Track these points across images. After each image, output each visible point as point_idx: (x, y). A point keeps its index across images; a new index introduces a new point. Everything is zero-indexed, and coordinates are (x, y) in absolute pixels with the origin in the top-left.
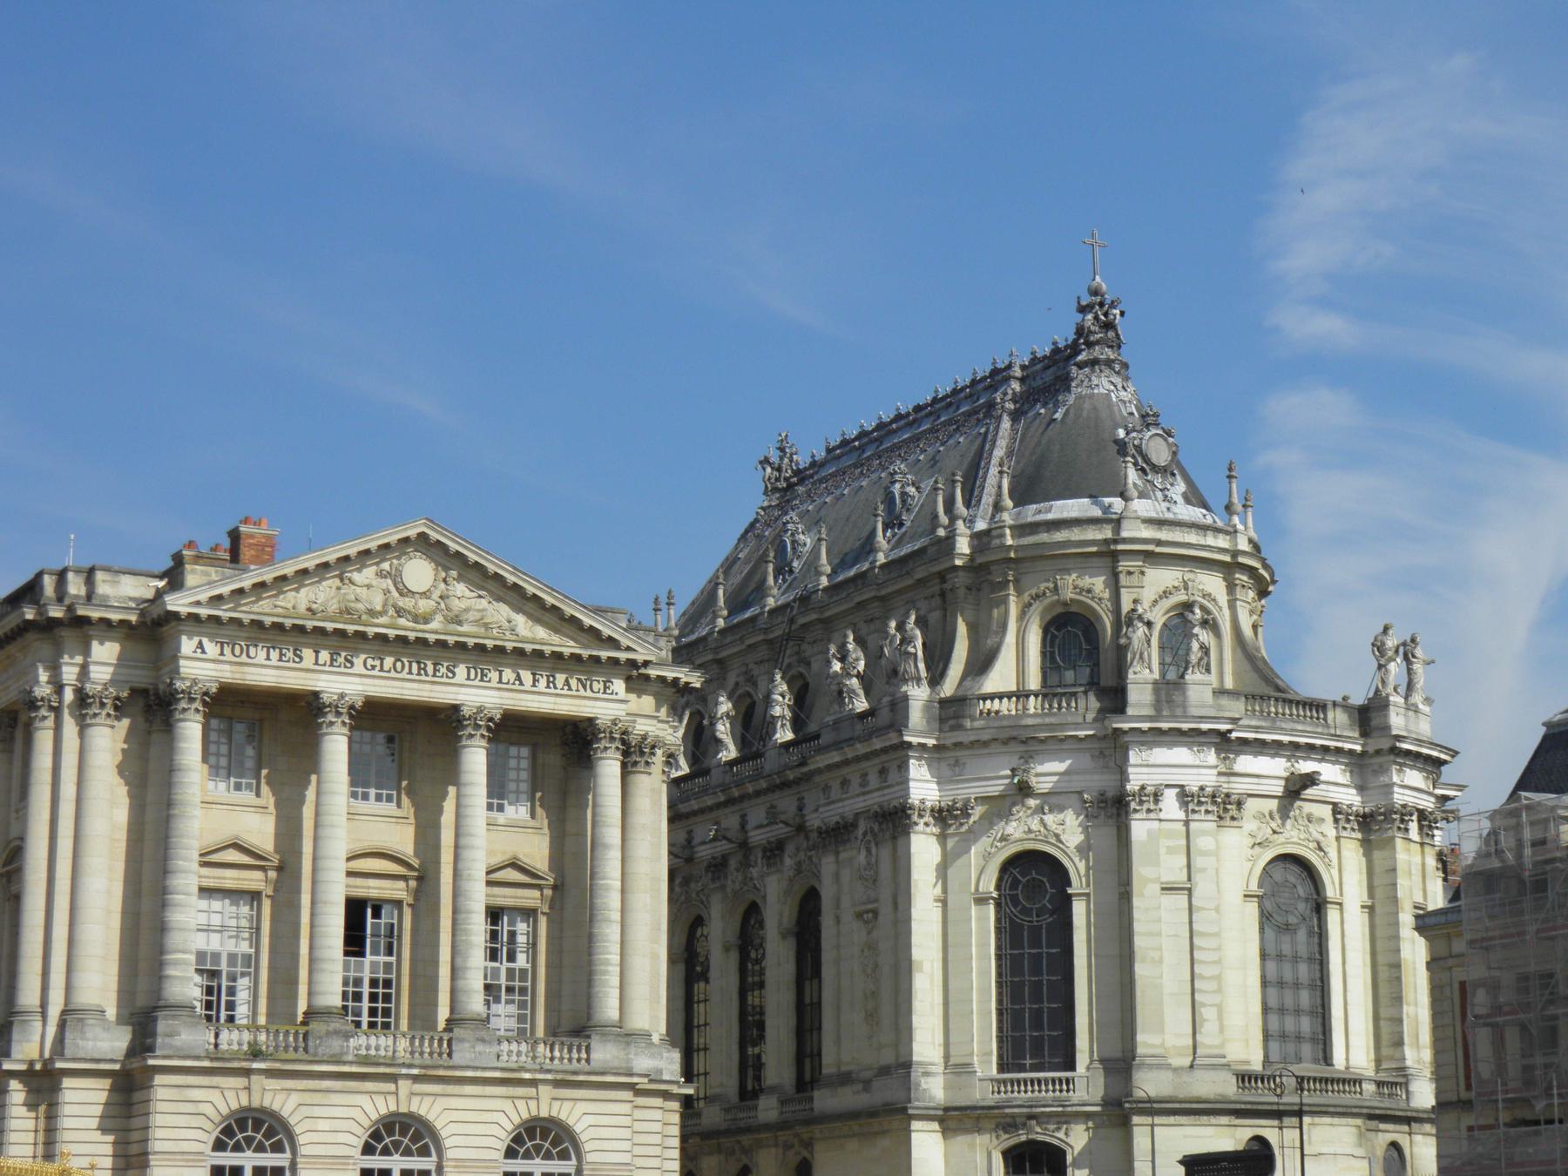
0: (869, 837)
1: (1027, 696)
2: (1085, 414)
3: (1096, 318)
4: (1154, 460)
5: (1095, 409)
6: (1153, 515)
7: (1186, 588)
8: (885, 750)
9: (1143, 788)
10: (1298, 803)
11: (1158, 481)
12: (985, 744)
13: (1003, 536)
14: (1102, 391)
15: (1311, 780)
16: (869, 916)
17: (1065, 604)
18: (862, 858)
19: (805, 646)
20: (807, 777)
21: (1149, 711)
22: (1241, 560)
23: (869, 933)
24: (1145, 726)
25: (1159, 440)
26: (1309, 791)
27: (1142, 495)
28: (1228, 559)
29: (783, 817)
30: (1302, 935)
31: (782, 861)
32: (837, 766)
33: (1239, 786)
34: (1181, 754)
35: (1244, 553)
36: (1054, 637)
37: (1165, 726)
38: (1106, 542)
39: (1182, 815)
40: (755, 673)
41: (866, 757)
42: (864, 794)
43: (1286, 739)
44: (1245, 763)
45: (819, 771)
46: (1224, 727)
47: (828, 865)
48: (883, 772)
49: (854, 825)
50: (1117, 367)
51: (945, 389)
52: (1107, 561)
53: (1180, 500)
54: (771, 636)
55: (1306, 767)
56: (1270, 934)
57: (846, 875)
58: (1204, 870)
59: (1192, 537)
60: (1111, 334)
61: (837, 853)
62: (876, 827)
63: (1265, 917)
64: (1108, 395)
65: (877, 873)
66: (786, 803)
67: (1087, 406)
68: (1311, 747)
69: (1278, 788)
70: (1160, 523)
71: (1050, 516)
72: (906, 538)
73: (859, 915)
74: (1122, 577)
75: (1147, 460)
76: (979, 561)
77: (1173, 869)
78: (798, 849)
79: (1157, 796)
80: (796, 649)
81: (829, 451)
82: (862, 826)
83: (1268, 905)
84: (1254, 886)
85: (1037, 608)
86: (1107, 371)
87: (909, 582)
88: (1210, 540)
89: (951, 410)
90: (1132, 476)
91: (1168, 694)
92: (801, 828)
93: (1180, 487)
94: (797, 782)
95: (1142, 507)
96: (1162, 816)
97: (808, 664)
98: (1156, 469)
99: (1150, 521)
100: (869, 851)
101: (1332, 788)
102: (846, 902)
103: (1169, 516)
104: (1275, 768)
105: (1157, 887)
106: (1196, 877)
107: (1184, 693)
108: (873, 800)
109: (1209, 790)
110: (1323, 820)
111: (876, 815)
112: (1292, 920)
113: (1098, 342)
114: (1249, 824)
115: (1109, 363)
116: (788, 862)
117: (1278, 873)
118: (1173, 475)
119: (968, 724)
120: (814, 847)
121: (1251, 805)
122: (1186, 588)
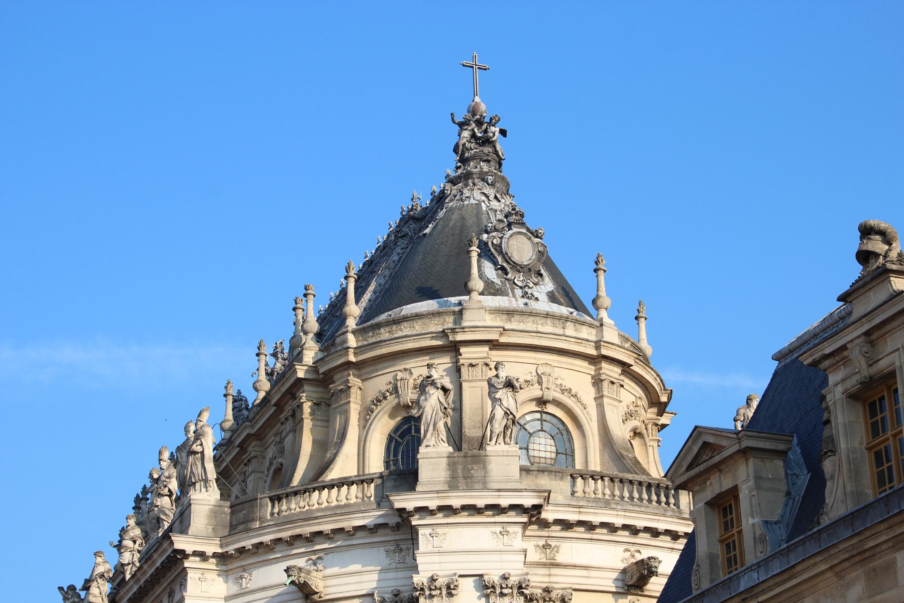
2: (451, 224)
3: (473, 136)
4: (516, 258)
5: (463, 219)
9: (433, 579)
11: (519, 279)
13: (345, 341)
14: (472, 201)
22: (604, 352)
28: (594, 352)
36: (398, 445)
37: (456, 503)
38: (444, 334)
44: (573, 549)
46: (528, 501)
64: (478, 205)
67: (455, 216)
74: (464, 370)
86: (480, 184)
107: (485, 468)
109: (513, 580)
113: (473, 158)
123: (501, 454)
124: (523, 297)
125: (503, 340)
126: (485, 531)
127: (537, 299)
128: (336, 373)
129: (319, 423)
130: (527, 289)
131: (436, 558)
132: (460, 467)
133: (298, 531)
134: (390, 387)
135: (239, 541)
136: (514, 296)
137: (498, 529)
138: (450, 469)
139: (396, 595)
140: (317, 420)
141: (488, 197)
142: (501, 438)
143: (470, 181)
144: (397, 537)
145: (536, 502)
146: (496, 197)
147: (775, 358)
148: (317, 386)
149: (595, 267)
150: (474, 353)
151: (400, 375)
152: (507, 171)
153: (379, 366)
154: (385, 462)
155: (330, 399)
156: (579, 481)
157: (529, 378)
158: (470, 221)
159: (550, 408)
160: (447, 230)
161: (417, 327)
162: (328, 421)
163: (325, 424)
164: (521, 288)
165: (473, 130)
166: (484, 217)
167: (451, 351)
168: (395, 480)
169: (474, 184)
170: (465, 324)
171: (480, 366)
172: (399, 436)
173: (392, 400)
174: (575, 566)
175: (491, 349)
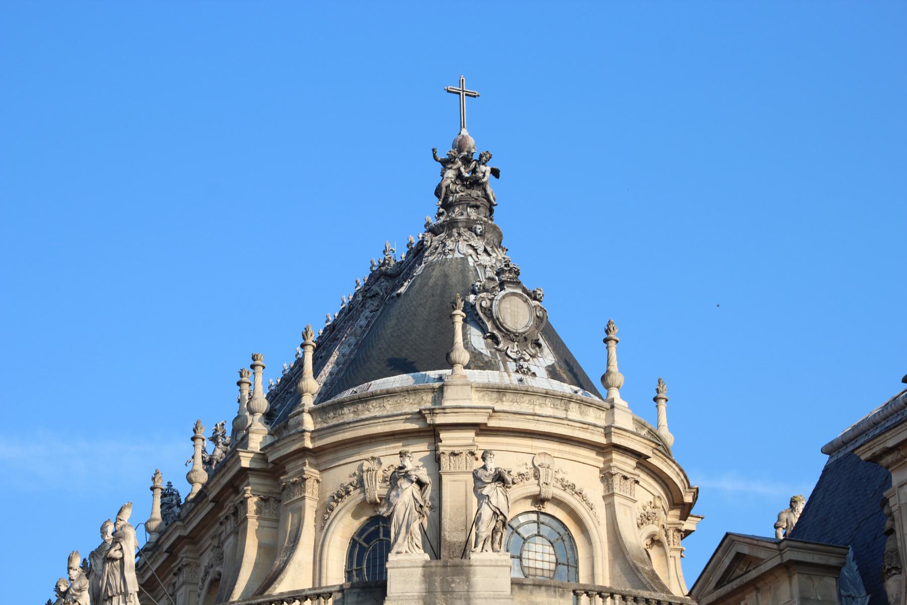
2: (431, 282)
3: (459, 176)
4: (509, 324)
5: (446, 276)
7: (537, 477)
11: (513, 350)
13: (301, 423)
14: (457, 255)
22: (615, 440)
28: (603, 440)
36: (362, 550)
38: (420, 415)
64: (464, 260)
67: (436, 273)
74: (444, 460)
86: (467, 234)
91: (444, 581)
107: (468, 580)
122: (537, 477)
123: (487, 563)
124: (517, 371)
125: (493, 423)
127: (534, 374)
128: (289, 462)
129: (266, 523)
132: (438, 579)
134: (354, 479)
136: (506, 370)
138: (425, 581)
140: (265, 519)
141: (475, 250)
142: (489, 543)
143: (455, 230)
146: (485, 251)
147: (825, 451)
148: (266, 477)
149: (605, 336)
150: (457, 439)
151: (366, 466)
153: (341, 454)
154: (346, 571)
155: (280, 494)
157: (523, 471)
158: (454, 279)
159: (549, 508)
160: (426, 289)
161: (388, 407)
162: (277, 521)
163: (274, 524)
164: (515, 360)
165: (459, 169)
166: (471, 274)
167: (430, 436)
168: (359, 595)
169: (459, 234)
170: (446, 404)
171: (464, 455)
172: (364, 540)
173: (356, 496)
175: (477, 435)
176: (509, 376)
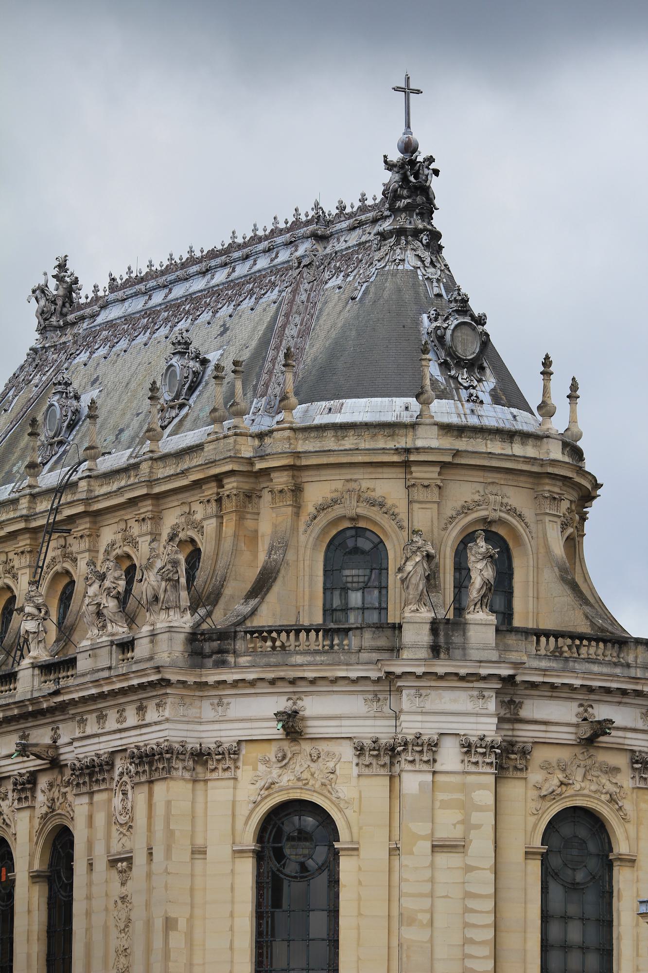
0: (125, 778)
1: (298, 632)
4: (460, 352)
6: (454, 420)
8: (142, 687)
10: (592, 751)
11: (463, 377)
12: (253, 683)
14: (408, 267)
15: (603, 728)
16: (121, 863)
17: (352, 519)
18: (117, 801)
19: (70, 540)
20: (62, 707)
21: (424, 653)
22: (550, 470)
23: (123, 884)
24: (419, 670)
25: (466, 330)
26: (602, 739)
27: (442, 395)
29: (35, 750)
30: (591, 897)
31: (34, 798)
32: (93, 698)
33: (526, 734)
34: (457, 700)
35: (554, 462)
37: (441, 670)
39: (459, 767)
40: (16, 563)
41: (123, 692)
42: (120, 731)
43: (577, 682)
44: (536, 708)
45: (73, 703)
46: (505, 672)
47: (80, 806)
48: (141, 709)
49: (111, 765)
50: (425, 239)
51: (244, 233)
52: (399, 472)
53: (486, 398)
54: (34, 524)
55: (601, 712)
56: (556, 891)
57: (100, 819)
58: (478, 827)
59: (496, 447)
60: (419, 199)
61: (91, 794)
62: (132, 768)
63: (548, 875)
65: (132, 819)
66: (42, 736)
68: (608, 691)
69: (566, 735)
70: (459, 430)
71: (338, 418)
72: (188, 423)
73: (113, 863)
75: (451, 353)
76: (259, 465)
77: (448, 825)
78: (51, 785)
79: (433, 746)
80: (62, 542)
81: (113, 286)
82: (120, 765)
83: (556, 862)
84: (537, 842)
85: (323, 520)
87: (185, 482)
88: (518, 449)
89: (250, 262)
90: (433, 369)
92: (55, 764)
93: (490, 382)
94: (51, 711)
95: (444, 410)
96: (438, 767)
97: (75, 560)
98: (461, 363)
99: (446, 428)
100: (125, 794)
101: (629, 735)
102: (99, 850)
103: (473, 421)
104: (563, 713)
105: (428, 845)
106: (473, 834)
108: (132, 739)
110: (616, 770)
111: (132, 756)
112: (580, 877)
114: (535, 776)
115: (416, 233)
116: (41, 798)
117: (567, 830)
118: (482, 369)
119: (231, 659)
120: (68, 783)
121: (540, 755)
124: (468, 401)
126: (463, 695)
127: (482, 402)
130: (472, 391)
131: (419, 718)
133: (282, 674)
135: (220, 674)
136: (460, 400)
137: (475, 693)
139: (374, 742)
141: (423, 262)
142: (479, 605)
144: (376, 688)
145: (511, 672)
146: (432, 263)
152: (438, 221)
156: (543, 639)
160: (381, 301)
163: (256, 517)
164: (466, 388)
168: (374, 633)
169: (407, 243)
174: (536, 722)
176: (462, 405)
